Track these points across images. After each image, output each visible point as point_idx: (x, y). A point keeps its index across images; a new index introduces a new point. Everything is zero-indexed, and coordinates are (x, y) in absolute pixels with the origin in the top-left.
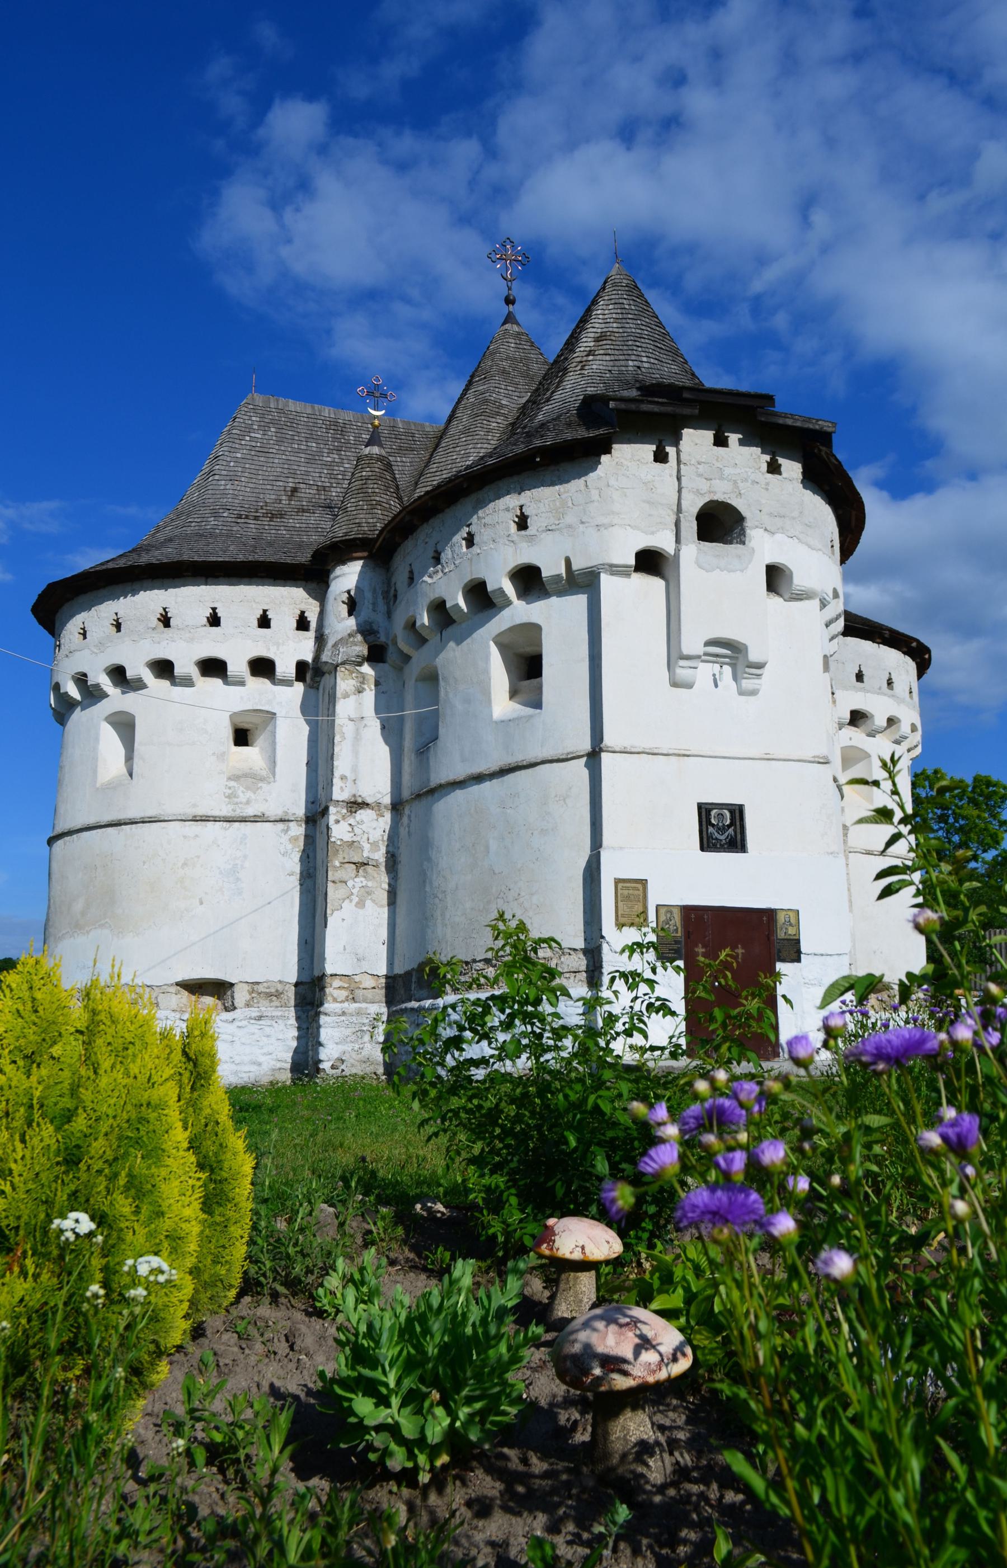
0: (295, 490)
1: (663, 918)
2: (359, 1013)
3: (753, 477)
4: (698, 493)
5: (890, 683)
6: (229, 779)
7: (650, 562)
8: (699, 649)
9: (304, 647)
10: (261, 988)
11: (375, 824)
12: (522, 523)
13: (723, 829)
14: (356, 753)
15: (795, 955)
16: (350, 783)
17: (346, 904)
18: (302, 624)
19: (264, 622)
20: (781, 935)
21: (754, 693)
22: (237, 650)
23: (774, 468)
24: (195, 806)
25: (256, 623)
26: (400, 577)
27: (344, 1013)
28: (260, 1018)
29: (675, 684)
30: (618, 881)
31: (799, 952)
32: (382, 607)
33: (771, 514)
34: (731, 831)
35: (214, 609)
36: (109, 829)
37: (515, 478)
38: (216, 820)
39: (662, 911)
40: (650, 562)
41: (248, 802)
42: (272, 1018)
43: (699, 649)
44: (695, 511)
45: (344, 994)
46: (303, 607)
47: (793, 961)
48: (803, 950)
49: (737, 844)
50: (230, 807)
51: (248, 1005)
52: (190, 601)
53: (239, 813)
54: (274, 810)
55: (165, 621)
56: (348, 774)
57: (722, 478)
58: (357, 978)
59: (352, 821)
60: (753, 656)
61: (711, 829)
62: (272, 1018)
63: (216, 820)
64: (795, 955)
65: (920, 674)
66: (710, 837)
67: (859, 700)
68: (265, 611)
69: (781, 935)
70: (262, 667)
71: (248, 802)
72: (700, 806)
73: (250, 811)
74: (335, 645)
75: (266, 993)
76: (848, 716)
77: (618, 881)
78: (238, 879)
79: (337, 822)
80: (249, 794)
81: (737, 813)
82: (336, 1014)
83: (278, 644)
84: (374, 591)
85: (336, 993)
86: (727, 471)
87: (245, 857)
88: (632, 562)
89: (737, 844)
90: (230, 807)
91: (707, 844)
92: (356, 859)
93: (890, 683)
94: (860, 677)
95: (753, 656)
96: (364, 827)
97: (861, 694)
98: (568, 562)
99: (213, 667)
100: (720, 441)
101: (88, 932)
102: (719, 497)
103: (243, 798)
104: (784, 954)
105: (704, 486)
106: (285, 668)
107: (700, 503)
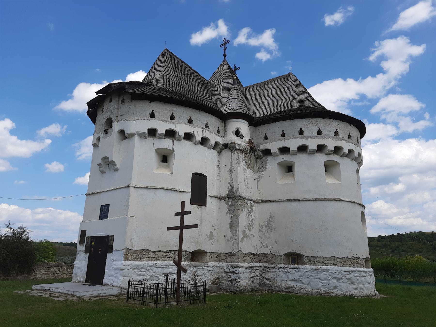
5: (301, 133)
8: (100, 161)
13: (104, 213)
21: (116, 170)
29: (103, 172)
31: (112, 250)
43: (100, 161)
44: (104, 123)
60: (110, 160)
76: (277, 150)
81: (108, 206)
94: (283, 135)
95: (110, 160)
97: (283, 142)
100: (111, 101)
107: (105, 120)
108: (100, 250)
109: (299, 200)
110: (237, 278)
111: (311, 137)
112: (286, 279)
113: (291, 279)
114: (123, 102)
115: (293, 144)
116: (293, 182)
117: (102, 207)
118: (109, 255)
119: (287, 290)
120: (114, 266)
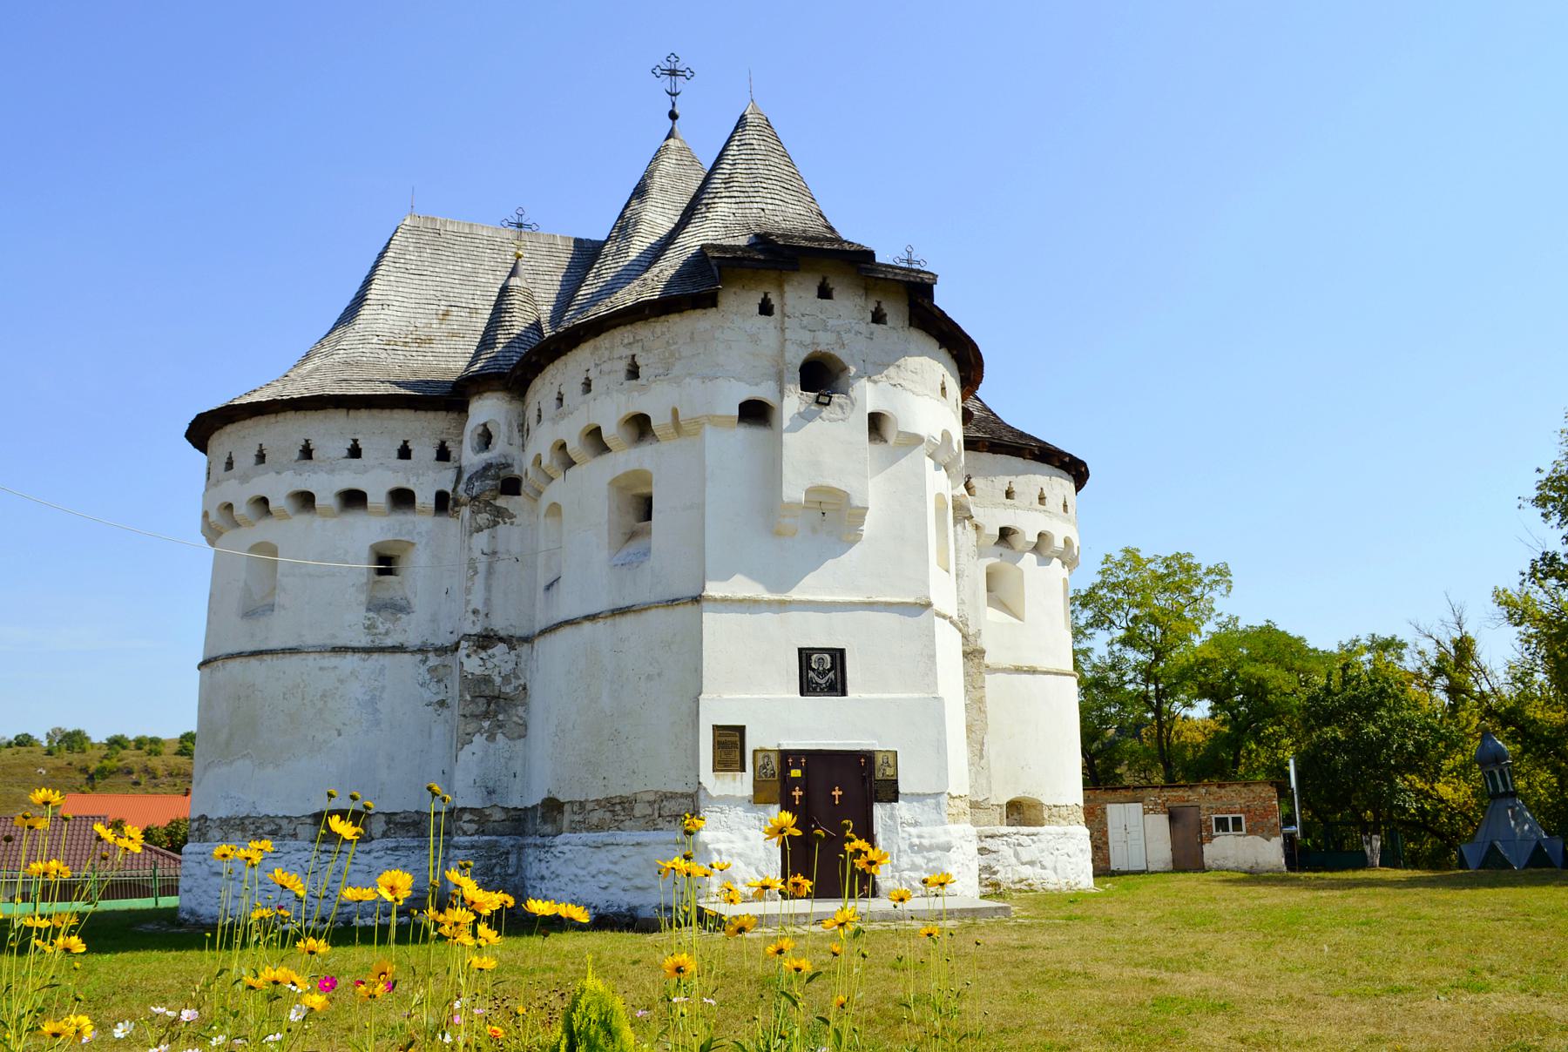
0: (446, 314)
1: (760, 763)
2: (492, 846)
3: (857, 327)
4: (801, 344)
5: (1042, 499)
6: (368, 610)
7: (755, 413)
9: (443, 479)
10: (398, 819)
11: (506, 657)
12: (633, 373)
13: (823, 673)
14: (488, 588)
15: (893, 796)
16: (481, 617)
17: (477, 739)
18: (443, 454)
19: (405, 453)
20: (879, 776)
22: (377, 481)
23: (878, 318)
24: (334, 636)
25: (396, 454)
26: (531, 415)
27: (473, 847)
28: (396, 849)
30: (716, 728)
31: (897, 792)
32: (517, 439)
33: (874, 363)
34: (831, 675)
35: (355, 441)
36: (253, 662)
37: (629, 327)
38: (354, 650)
39: (760, 755)
40: (755, 413)
41: (387, 633)
42: (409, 848)
45: (475, 826)
46: (444, 437)
47: (890, 801)
48: (901, 790)
49: (837, 687)
50: (369, 638)
51: (385, 835)
52: (331, 433)
53: (377, 643)
54: (412, 640)
55: (307, 453)
56: (480, 607)
57: (826, 330)
58: (488, 812)
59: (483, 655)
61: (811, 674)
62: (409, 848)
63: (354, 650)
64: (893, 796)
65: (1078, 489)
66: (810, 681)
67: (1007, 518)
68: (405, 442)
69: (879, 776)
70: (402, 499)
71: (387, 633)
72: (800, 650)
73: (389, 642)
74: (470, 479)
75: (403, 825)
77: (716, 728)
78: (377, 710)
79: (468, 656)
80: (388, 625)
81: (838, 656)
82: (465, 848)
83: (418, 476)
84: (510, 425)
85: (466, 826)
86: (831, 322)
87: (384, 687)
88: (737, 413)
89: (837, 687)
90: (369, 638)
91: (807, 688)
92: (487, 692)
93: (1042, 499)
96: (495, 660)
97: (1011, 511)
98: (675, 413)
99: (353, 499)
101: (232, 762)
102: (823, 348)
103: (381, 629)
104: (880, 796)
105: (807, 337)
106: (425, 498)
107: (803, 355)
108: (837, 793)
109: (1033, 671)
110: (993, 863)
111: (1056, 515)
112: (1013, 860)
113: (1025, 858)
114: (878, 318)
115: (1029, 524)
116: (1015, 620)
117: (805, 655)
118: (879, 811)
119: (1018, 886)
120: (916, 841)
